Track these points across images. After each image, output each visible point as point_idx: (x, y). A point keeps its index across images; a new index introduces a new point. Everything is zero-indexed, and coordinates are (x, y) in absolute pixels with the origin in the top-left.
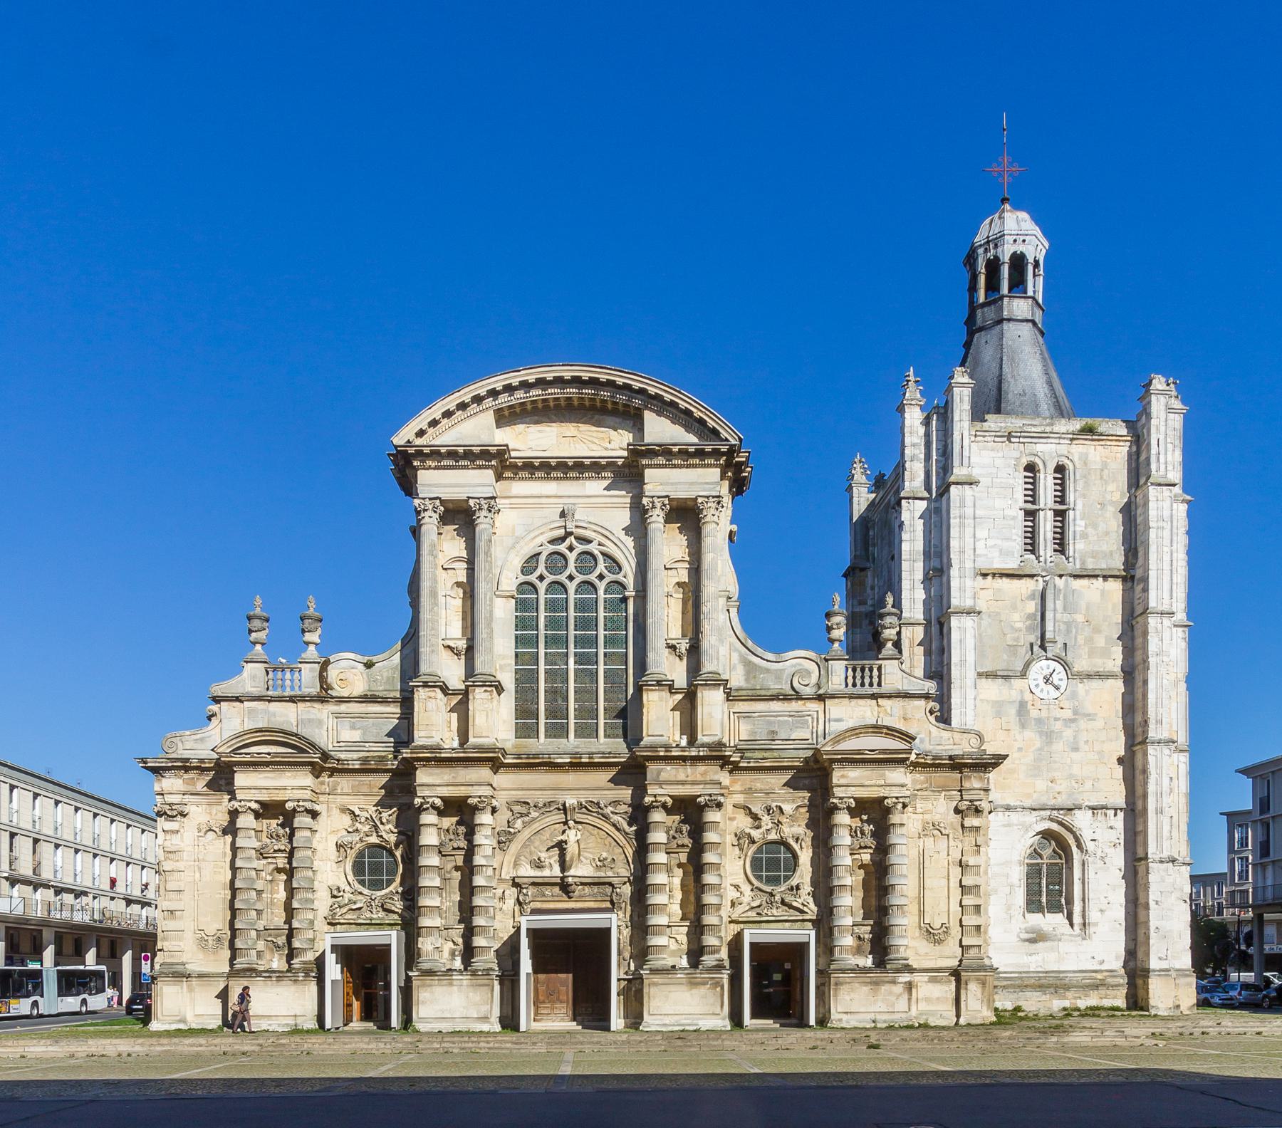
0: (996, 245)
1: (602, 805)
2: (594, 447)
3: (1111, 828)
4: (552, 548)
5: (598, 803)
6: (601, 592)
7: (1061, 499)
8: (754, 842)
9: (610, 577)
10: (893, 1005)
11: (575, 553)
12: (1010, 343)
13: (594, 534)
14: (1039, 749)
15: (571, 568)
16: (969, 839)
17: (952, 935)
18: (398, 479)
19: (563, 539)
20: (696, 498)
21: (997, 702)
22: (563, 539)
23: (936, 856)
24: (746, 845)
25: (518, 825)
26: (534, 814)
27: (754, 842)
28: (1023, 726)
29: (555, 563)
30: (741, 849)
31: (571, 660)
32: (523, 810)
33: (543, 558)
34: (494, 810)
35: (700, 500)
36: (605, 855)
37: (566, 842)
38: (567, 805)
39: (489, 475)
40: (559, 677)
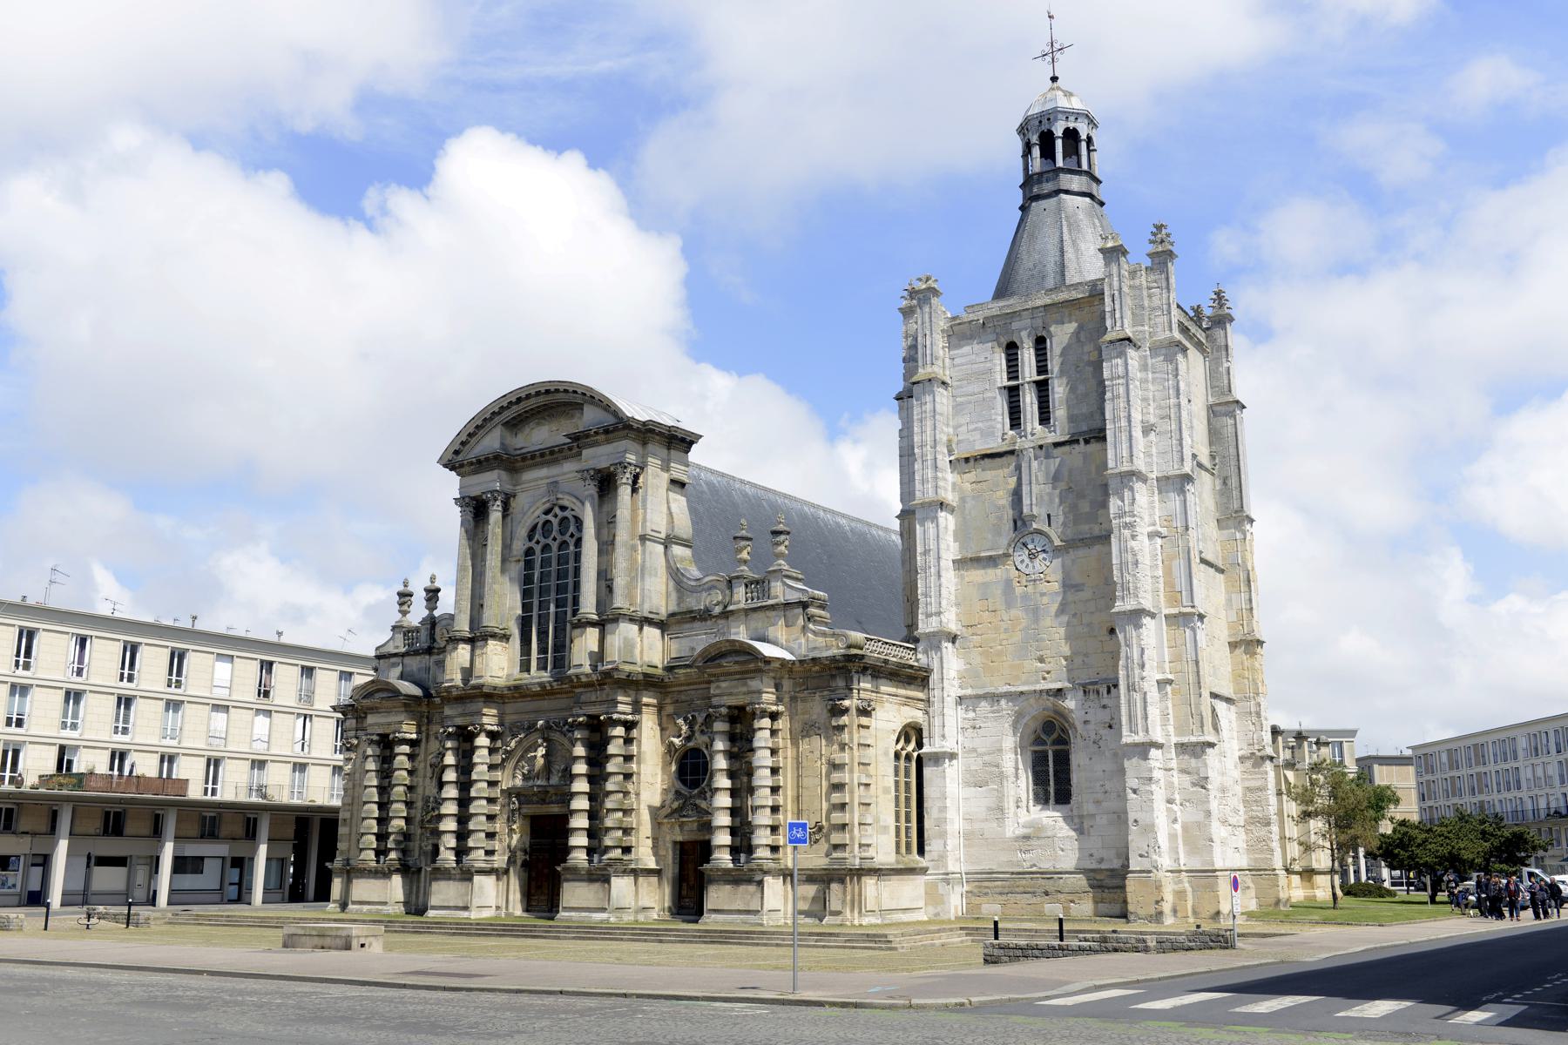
3: (1104, 707)
7: (1042, 368)
10: (748, 905)
21: (983, 584)
23: (810, 755)
28: (1009, 605)
33: (540, 526)
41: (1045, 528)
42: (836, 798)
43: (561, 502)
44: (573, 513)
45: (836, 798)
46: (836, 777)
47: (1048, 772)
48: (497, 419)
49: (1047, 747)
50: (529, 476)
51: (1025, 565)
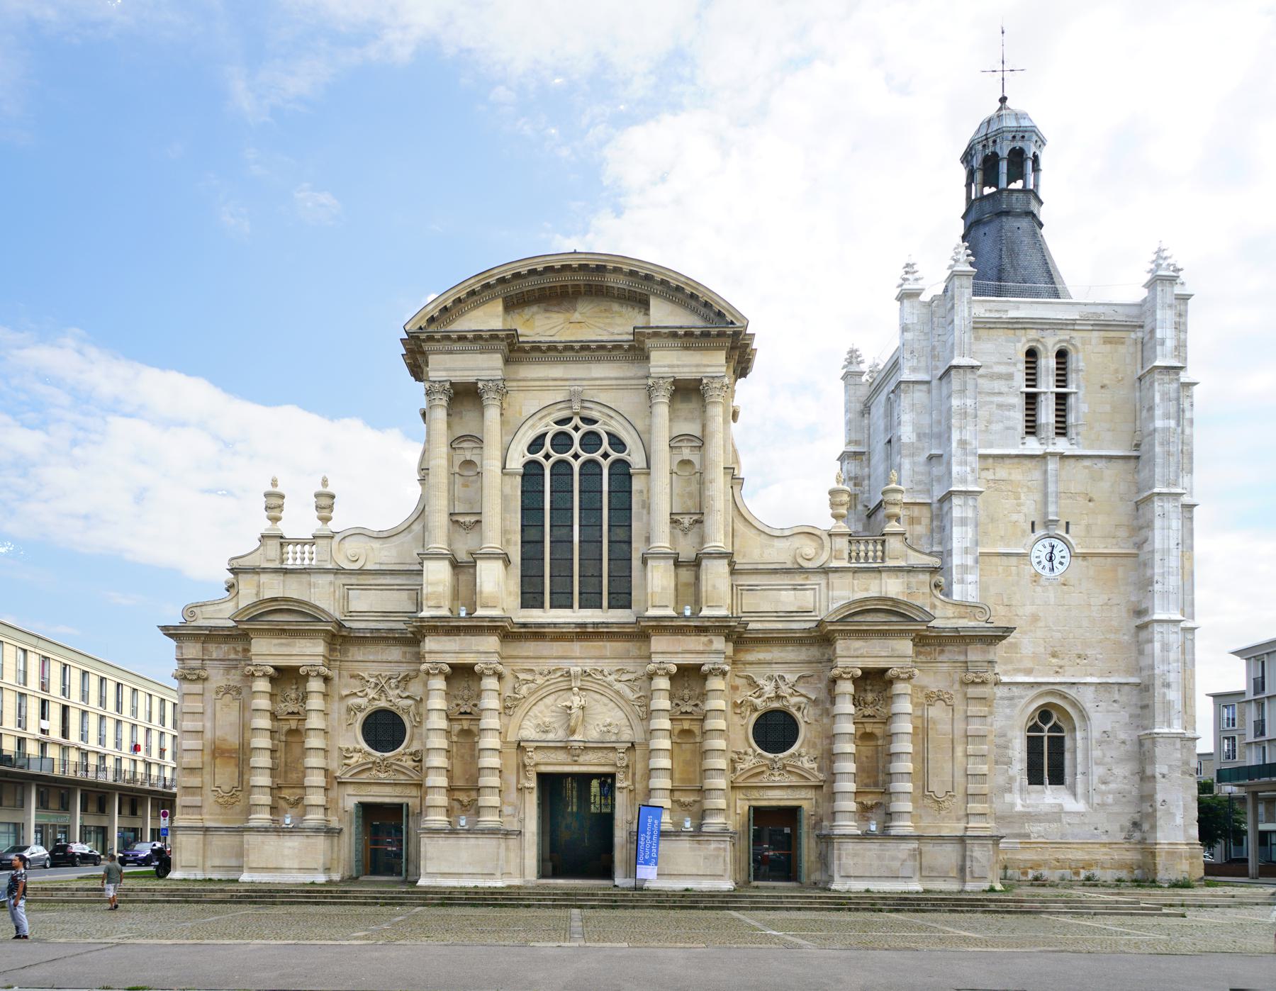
0: (995, 142)
1: (606, 673)
2: (600, 332)
5: (602, 672)
8: (756, 710)
9: (614, 455)
11: (580, 433)
12: (1009, 234)
13: (599, 414)
15: (576, 446)
18: (409, 365)
19: (569, 420)
20: (701, 380)
22: (566, 421)
24: (748, 713)
25: (524, 690)
26: (540, 680)
27: (756, 710)
29: (562, 442)
32: (530, 677)
34: (500, 677)
35: (705, 381)
36: (608, 720)
37: (570, 708)
38: (572, 672)
39: (496, 360)
41: (1063, 533)
43: (587, 413)
44: (607, 428)
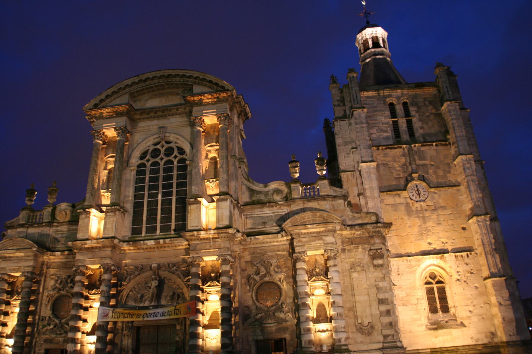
4: (154, 147)
6: (175, 163)
9: (180, 156)
14: (420, 226)
16: (378, 274)
17: (376, 329)
29: (156, 153)
30: (250, 286)
31: (160, 196)
40: (153, 205)
42: (383, 308)
43: (167, 139)
44: (176, 145)
45: (383, 308)
46: (381, 296)
47: (435, 298)
48: (127, 90)
49: (433, 286)
50: (142, 124)
51: (414, 197)
